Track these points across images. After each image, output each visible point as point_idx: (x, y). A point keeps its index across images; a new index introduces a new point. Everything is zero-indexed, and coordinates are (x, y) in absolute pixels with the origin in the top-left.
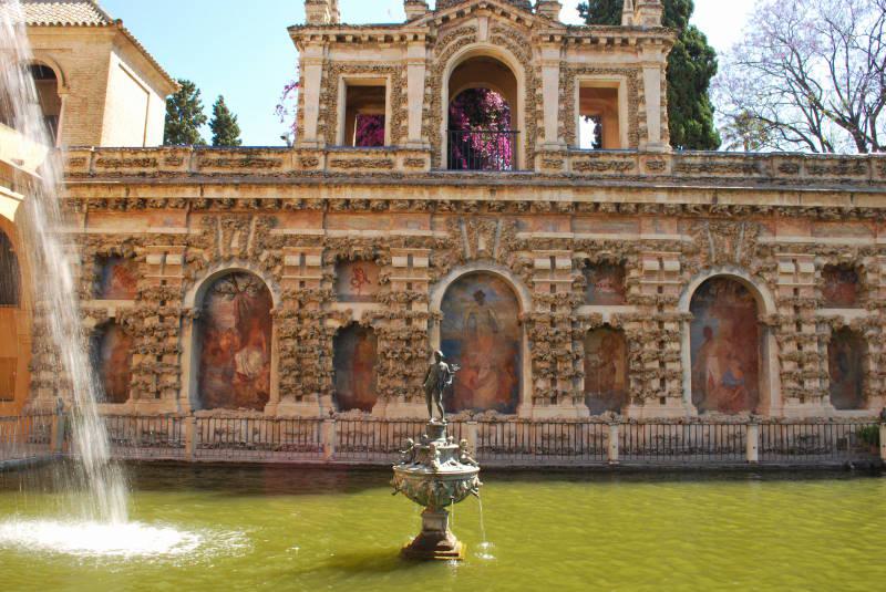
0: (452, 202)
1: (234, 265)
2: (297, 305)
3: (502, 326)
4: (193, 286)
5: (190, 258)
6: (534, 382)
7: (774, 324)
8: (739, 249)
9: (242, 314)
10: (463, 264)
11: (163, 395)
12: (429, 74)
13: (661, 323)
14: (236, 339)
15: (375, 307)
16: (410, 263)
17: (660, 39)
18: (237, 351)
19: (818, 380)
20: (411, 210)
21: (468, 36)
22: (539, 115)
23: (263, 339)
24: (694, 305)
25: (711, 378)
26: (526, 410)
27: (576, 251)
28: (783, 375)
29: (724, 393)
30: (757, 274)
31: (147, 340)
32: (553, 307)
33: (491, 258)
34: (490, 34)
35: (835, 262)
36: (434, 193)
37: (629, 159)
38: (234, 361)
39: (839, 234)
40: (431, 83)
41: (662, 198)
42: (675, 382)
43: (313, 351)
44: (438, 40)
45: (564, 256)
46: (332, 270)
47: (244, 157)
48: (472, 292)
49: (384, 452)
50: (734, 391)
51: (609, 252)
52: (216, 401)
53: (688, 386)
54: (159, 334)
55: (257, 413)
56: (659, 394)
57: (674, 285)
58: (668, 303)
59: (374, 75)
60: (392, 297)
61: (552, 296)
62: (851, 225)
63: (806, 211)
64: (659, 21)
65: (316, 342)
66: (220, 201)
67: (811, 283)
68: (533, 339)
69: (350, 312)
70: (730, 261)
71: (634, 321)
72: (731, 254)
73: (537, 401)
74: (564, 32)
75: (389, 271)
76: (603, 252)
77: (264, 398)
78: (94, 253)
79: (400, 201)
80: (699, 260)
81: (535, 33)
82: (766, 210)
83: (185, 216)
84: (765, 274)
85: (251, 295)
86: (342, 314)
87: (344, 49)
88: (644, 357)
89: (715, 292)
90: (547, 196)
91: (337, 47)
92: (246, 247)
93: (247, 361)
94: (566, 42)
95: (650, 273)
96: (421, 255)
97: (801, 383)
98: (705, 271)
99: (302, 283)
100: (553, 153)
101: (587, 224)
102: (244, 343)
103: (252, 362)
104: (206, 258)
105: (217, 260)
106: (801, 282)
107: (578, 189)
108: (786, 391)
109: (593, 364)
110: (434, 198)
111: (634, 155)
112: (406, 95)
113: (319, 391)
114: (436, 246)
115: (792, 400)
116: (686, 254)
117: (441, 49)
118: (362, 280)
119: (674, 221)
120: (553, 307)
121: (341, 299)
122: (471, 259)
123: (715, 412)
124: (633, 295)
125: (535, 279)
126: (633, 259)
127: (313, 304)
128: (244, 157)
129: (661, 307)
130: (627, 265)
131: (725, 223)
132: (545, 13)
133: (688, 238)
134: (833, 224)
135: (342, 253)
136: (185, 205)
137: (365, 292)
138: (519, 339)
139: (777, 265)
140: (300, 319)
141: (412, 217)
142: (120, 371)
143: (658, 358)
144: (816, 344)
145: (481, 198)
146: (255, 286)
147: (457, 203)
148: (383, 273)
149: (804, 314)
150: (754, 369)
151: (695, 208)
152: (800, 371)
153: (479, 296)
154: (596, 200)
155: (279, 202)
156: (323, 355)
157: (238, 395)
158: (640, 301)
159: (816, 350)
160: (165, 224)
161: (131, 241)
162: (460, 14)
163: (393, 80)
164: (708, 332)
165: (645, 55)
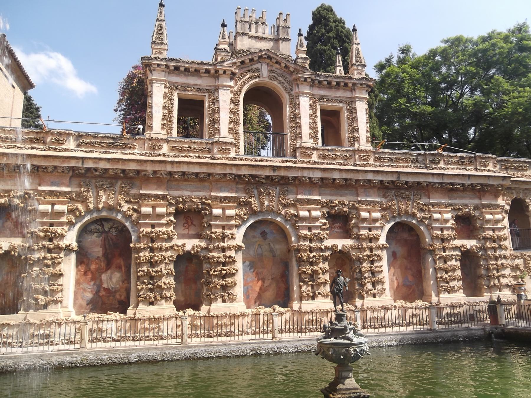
0: (250, 175)
1: (104, 214)
2: (150, 240)
3: (278, 253)
6: (300, 287)
9: (107, 246)
12: (232, 95)
14: (103, 264)
17: (365, 84)
18: (102, 273)
20: (224, 180)
22: (298, 126)
23: (122, 263)
24: (388, 239)
26: (296, 306)
27: (323, 207)
30: (421, 220)
35: (460, 213)
36: (239, 170)
38: (101, 280)
39: (462, 198)
41: (370, 177)
43: (161, 271)
45: (316, 210)
46: (172, 218)
47: (111, 141)
48: (259, 231)
49: (211, 337)
51: (341, 208)
52: (86, 309)
53: (387, 286)
54: (49, 262)
55: (122, 315)
56: (372, 292)
60: (213, 235)
61: (309, 234)
62: (468, 193)
65: (163, 265)
66: (96, 170)
67: (449, 225)
69: (184, 245)
73: (303, 299)
74: (313, 77)
75: (209, 219)
81: (294, 76)
82: (425, 184)
83: (68, 179)
85: (114, 234)
86: (180, 246)
87: (178, 75)
89: (397, 231)
91: (173, 73)
93: (112, 279)
96: (230, 208)
97: (448, 283)
99: (153, 226)
100: (308, 148)
102: (108, 266)
103: (114, 280)
110: (239, 172)
112: (219, 107)
118: (190, 224)
119: (376, 190)
120: (311, 241)
122: (261, 212)
123: (403, 302)
124: (355, 234)
128: (111, 141)
134: (459, 192)
136: (69, 171)
137: (192, 232)
138: (289, 261)
140: (152, 250)
144: (454, 260)
145: (268, 174)
146: (117, 228)
151: (388, 183)
152: (447, 276)
153: (264, 234)
154: (334, 177)
155: (138, 172)
157: (103, 303)
160: (53, 184)
162: (252, 60)
163: (210, 98)
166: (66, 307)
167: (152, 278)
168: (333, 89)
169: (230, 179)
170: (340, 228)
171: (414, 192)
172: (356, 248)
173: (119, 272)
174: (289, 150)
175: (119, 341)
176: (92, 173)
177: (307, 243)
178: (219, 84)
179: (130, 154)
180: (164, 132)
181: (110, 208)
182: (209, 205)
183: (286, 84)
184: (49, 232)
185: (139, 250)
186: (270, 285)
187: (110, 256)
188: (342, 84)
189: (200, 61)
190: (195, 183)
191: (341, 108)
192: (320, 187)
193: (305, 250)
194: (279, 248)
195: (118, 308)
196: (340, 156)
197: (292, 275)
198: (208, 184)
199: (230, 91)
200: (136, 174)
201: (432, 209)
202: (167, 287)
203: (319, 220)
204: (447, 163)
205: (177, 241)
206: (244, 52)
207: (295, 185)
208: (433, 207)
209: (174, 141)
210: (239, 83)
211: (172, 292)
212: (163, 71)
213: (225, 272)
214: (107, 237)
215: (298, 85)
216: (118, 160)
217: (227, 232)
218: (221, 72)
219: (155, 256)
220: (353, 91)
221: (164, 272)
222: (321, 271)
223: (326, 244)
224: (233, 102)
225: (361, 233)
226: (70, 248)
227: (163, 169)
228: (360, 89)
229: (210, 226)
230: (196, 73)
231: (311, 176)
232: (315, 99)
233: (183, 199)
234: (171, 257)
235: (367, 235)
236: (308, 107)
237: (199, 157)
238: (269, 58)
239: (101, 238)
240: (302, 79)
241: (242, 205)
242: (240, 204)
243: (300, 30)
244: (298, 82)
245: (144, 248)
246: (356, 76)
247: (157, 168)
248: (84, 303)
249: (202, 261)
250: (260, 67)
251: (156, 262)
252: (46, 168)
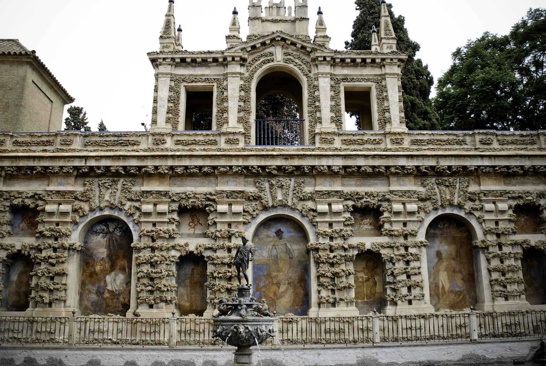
0: (259, 166)
1: (107, 212)
2: (150, 239)
3: (296, 254)
4: (77, 228)
5: (77, 207)
6: (319, 292)
7: (484, 246)
8: (456, 195)
9: (111, 247)
10: (267, 210)
11: (53, 305)
12: (242, 82)
13: (406, 248)
14: (107, 266)
15: (207, 242)
16: (230, 210)
17: (395, 58)
18: (107, 274)
19: (516, 284)
21: (269, 58)
22: (318, 109)
23: (126, 265)
25: (443, 287)
26: (313, 312)
27: (346, 200)
28: (492, 283)
29: (452, 296)
31: (43, 266)
32: (331, 238)
33: (285, 206)
34: (283, 57)
35: (521, 202)
37: (380, 138)
38: (105, 282)
39: (523, 184)
40: (245, 89)
41: (402, 162)
42: (418, 289)
43: (161, 273)
44: (248, 61)
45: (337, 202)
46: (175, 216)
47: (116, 139)
50: (460, 295)
52: (91, 310)
54: (54, 261)
56: (407, 298)
57: (414, 221)
58: (411, 234)
59: (205, 84)
60: (218, 234)
62: (531, 178)
63: (499, 169)
64: (394, 47)
65: (164, 266)
66: (99, 168)
67: (506, 217)
68: (318, 263)
69: (187, 245)
70: (451, 205)
71: (388, 247)
72: (452, 196)
73: (321, 306)
74: (332, 55)
75: (214, 216)
76: (365, 200)
77: (126, 307)
78: (8, 204)
79: (224, 167)
80: (429, 205)
81: (312, 55)
82: (473, 168)
84: (475, 213)
85: (118, 234)
86: (182, 246)
88: (396, 272)
90: (325, 162)
91: (180, 66)
92: (115, 199)
93: (114, 281)
94: (334, 61)
95: (398, 213)
96: (237, 203)
97: (505, 287)
98: (435, 212)
99: (154, 224)
101: (353, 181)
102: (113, 268)
103: (118, 282)
104: (86, 207)
105: (92, 210)
106: (500, 217)
107: (345, 157)
108: (495, 294)
109: (360, 280)
111: (383, 134)
113: (166, 301)
114: (249, 199)
115: (499, 299)
116: (422, 200)
117: (250, 67)
120: (331, 238)
121: (182, 235)
122: (273, 207)
123: (448, 310)
124: (386, 230)
125: (318, 219)
126: (385, 204)
127: (162, 240)
128: (116, 139)
129: (406, 237)
130: (381, 209)
131: (446, 179)
132: (320, 43)
133: (421, 189)
134: (519, 178)
135: (184, 202)
136: (73, 171)
137: (198, 232)
139: (483, 205)
140: (153, 249)
141: (231, 178)
142: (23, 289)
143: (406, 272)
144: (513, 259)
147: (263, 168)
148: (211, 217)
149: (503, 240)
150: (472, 279)
152: (503, 278)
153: (279, 234)
155: (140, 168)
156: (168, 275)
157: (108, 306)
158: (393, 233)
159: (514, 263)
160: (60, 184)
161: (36, 196)
162: (264, 44)
163: (218, 87)
164: (439, 254)
165: (388, 70)
166: (69, 307)
167: (152, 279)
168: (359, 68)
169: (237, 172)
170: (370, 224)
171: (460, 179)
172: (388, 247)
173: (123, 274)
174: (307, 136)
175: (118, 343)
176: (95, 171)
177: (327, 241)
178: (229, 71)
179: (133, 150)
180: (169, 126)
181: (112, 207)
182: (214, 201)
183: (304, 66)
184: (54, 231)
185: (139, 250)
186: (287, 290)
187: (114, 257)
188: (369, 61)
189: (206, 50)
190: (200, 178)
191: (370, 88)
192: (343, 177)
193: (325, 250)
194: (297, 248)
195: (122, 311)
196: (367, 141)
197: (310, 279)
198: (214, 179)
199: (239, 78)
200: (137, 171)
201: (484, 198)
202: (168, 290)
203: (341, 215)
204: (502, 143)
205: (180, 241)
206: (256, 37)
207: (314, 177)
208: (485, 195)
209: (178, 135)
210: (251, 69)
211: (174, 295)
212: (169, 65)
213: (230, 274)
214: (112, 237)
215: (317, 66)
216: (118, 157)
217: (234, 229)
218: (229, 59)
219: (155, 256)
220: (383, 68)
221: (165, 273)
222: (343, 274)
223: (350, 243)
224: (243, 90)
225: (393, 229)
226: (74, 247)
227: (164, 164)
228: (391, 64)
229: (215, 223)
230: (204, 63)
231: (330, 163)
232: (336, 81)
233: (187, 196)
234: (173, 257)
235: (400, 231)
236: (328, 88)
237: (204, 150)
238: (284, 39)
239: (106, 239)
240: (320, 59)
241: (251, 200)
242: (249, 199)
243: (320, 8)
244: (317, 62)
245: (144, 248)
246: (386, 51)
247: (157, 163)
248: (89, 305)
249: (206, 262)
250: (274, 51)
251: (157, 263)
252: (53, 168)
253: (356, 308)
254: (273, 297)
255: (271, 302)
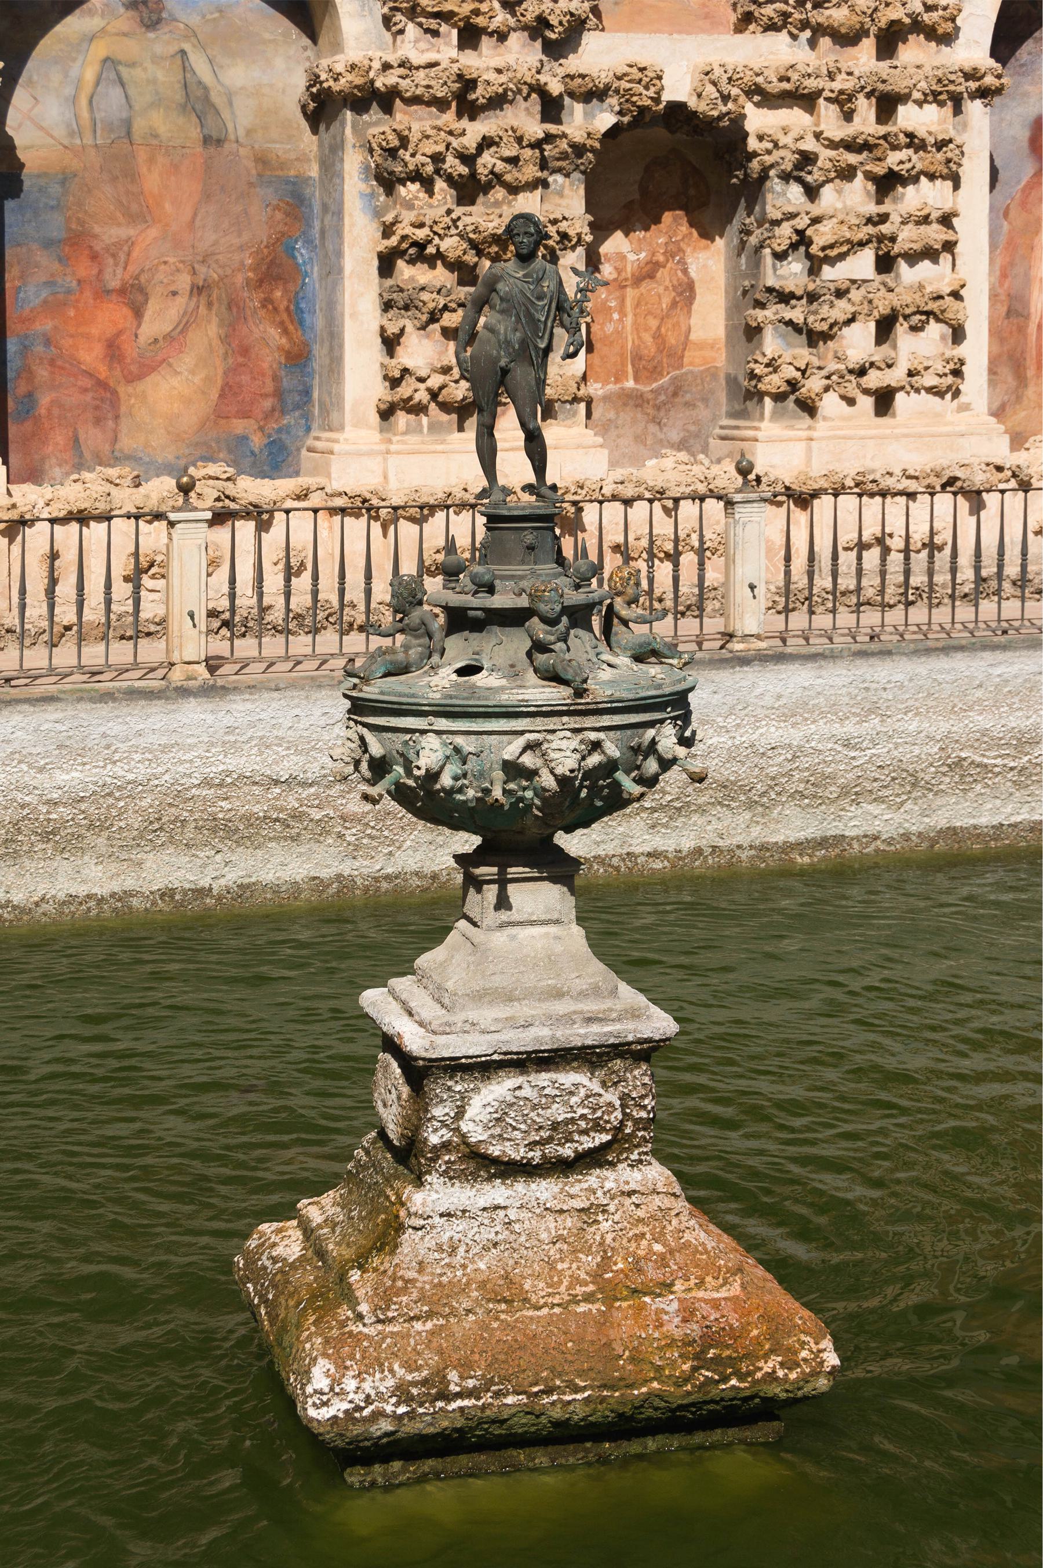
53: (976, 351)
58: (917, 26)
88: (822, 236)
186: (184, 327)
253: (589, 436)
254: (103, 371)
255: (88, 397)
